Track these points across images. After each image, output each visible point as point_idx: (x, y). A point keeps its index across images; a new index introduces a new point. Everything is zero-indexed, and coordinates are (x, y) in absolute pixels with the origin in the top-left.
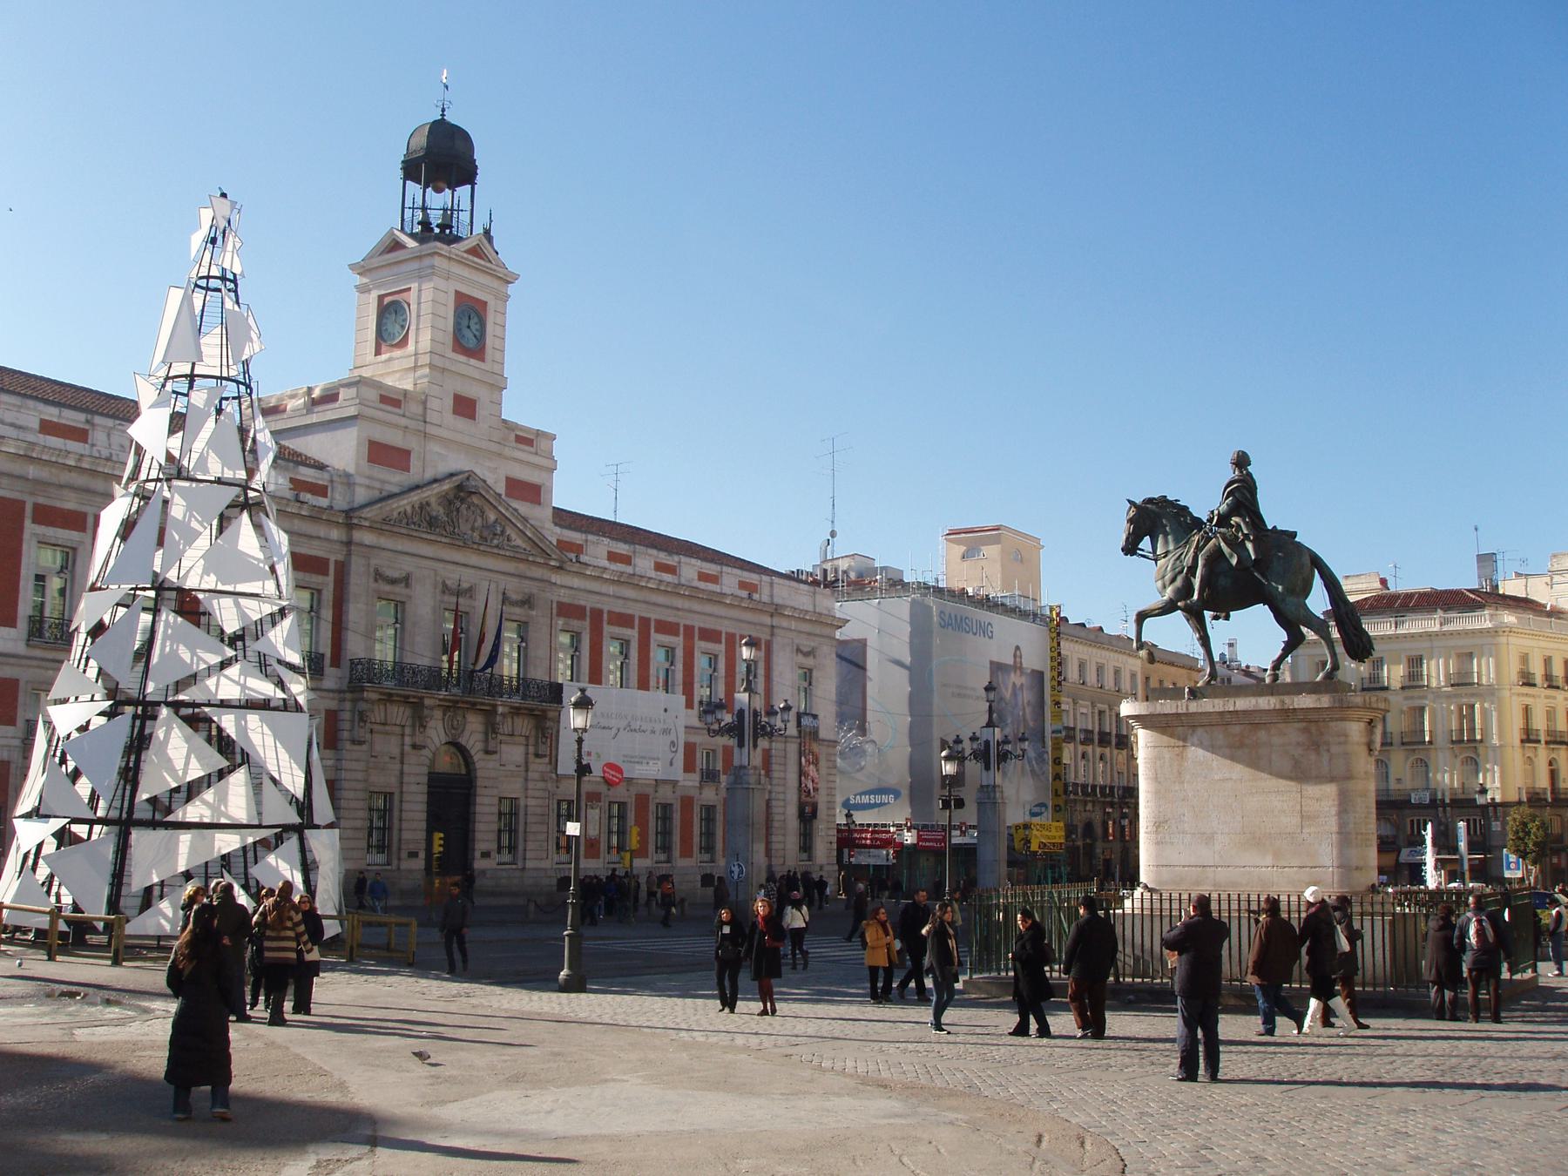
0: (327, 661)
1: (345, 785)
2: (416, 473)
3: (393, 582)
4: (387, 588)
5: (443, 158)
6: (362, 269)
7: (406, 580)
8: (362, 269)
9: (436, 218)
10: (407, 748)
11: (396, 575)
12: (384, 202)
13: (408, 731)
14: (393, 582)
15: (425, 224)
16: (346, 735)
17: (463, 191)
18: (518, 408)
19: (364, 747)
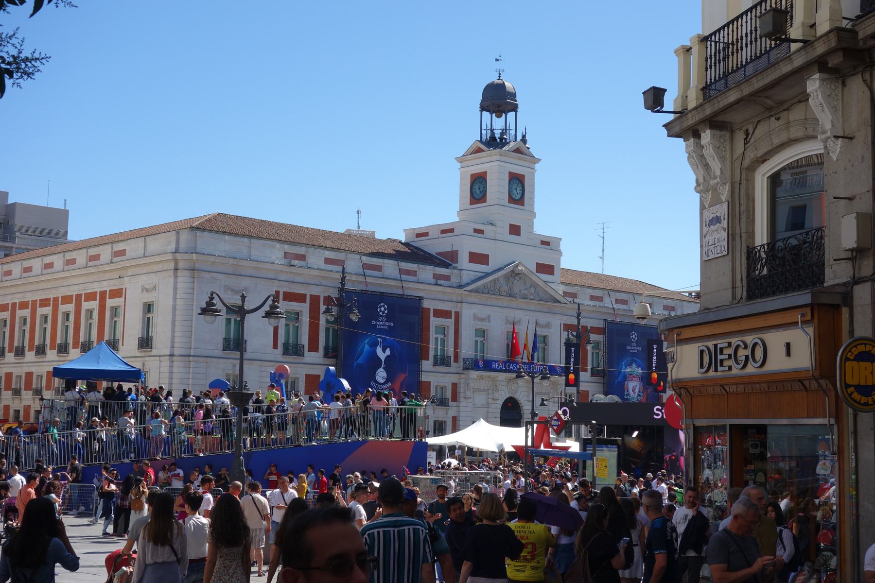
0: (452, 359)
1: (461, 418)
2: (493, 264)
3: (482, 320)
4: (479, 323)
5: (498, 99)
6: (460, 160)
7: (488, 319)
8: (460, 160)
9: (497, 135)
10: (490, 401)
11: (484, 316)
12: (472, 124)
13: (490, 392)
14: (482, 320)
15: (493, 138)
16: (462, 395)
17: (511, 115)
18: (542, 227)
19: (470, 400)
